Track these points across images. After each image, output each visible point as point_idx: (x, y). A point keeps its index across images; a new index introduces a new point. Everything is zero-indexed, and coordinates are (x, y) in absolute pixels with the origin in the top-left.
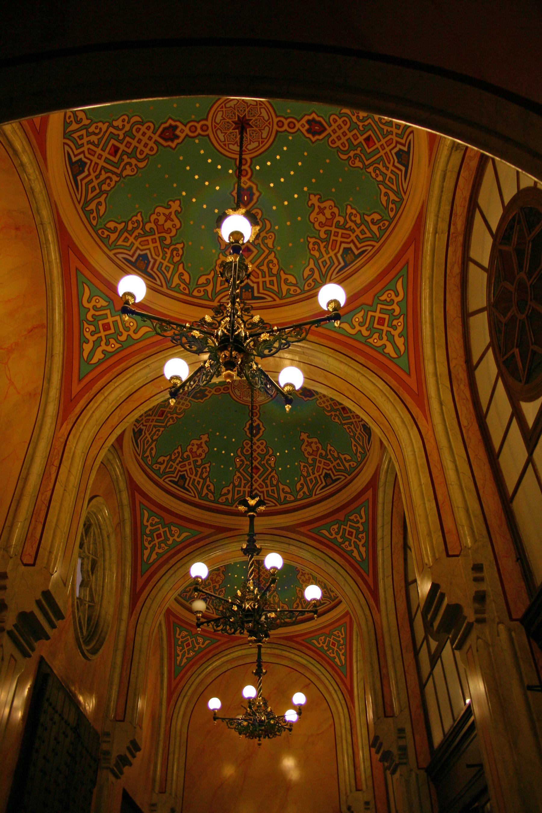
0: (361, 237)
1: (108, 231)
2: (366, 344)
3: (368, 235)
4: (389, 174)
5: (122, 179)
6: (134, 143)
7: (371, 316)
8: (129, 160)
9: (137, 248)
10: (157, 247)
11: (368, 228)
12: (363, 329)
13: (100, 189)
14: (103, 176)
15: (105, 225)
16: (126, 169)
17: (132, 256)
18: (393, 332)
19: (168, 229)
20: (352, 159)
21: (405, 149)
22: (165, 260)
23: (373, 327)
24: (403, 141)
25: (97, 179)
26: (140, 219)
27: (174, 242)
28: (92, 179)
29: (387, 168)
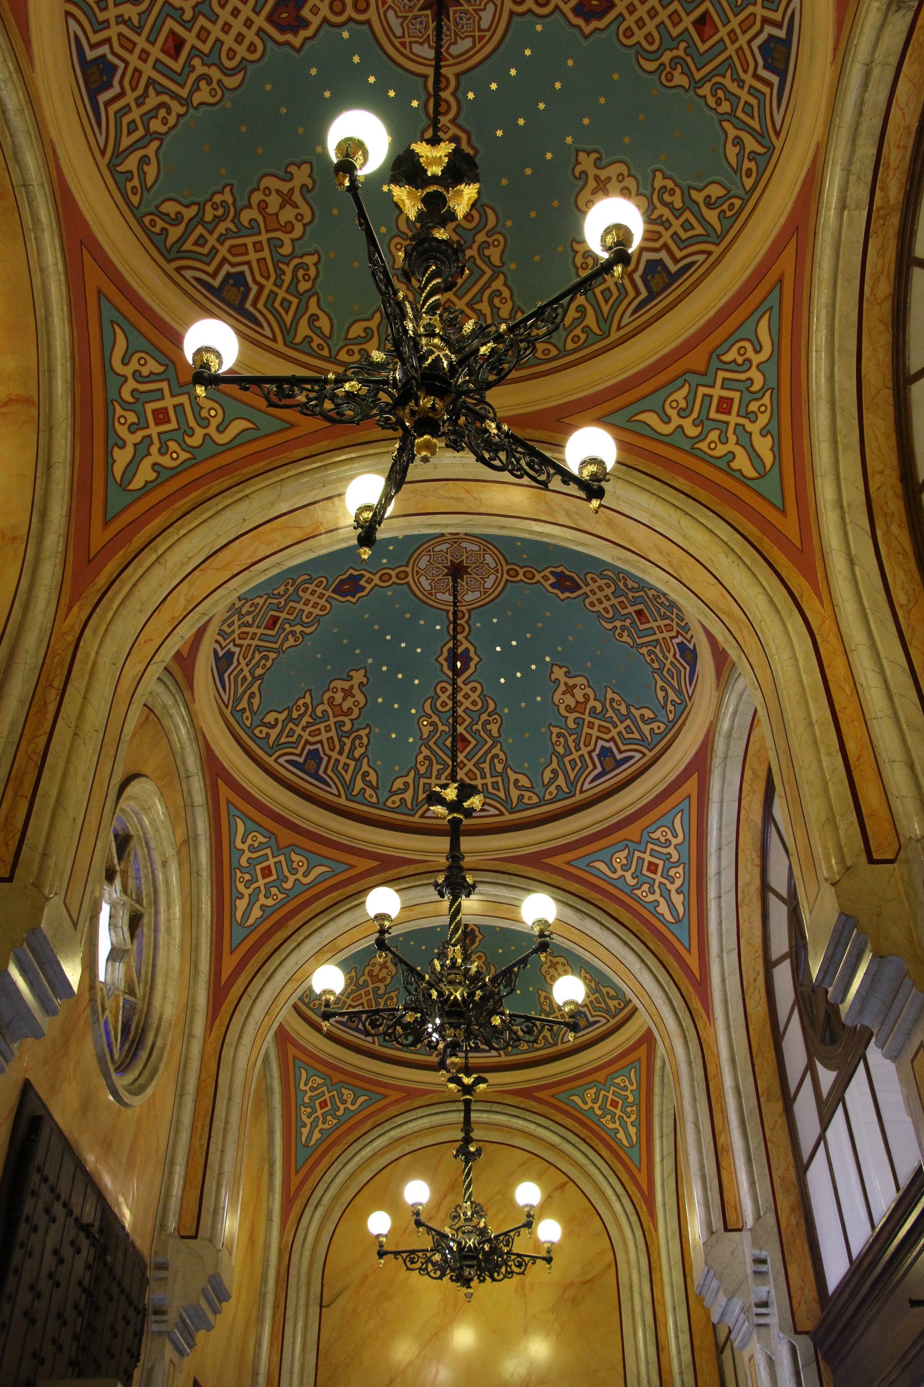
0: (684, 235)
1: (163, 220)
2: (693, 452)
3: (699, 230)
4: (744, 95)
5: (191, 110)
6: (216, 31)
7: (704, 395)
8: (205, 70)
9: (224, 260)
10: (264, 259)
11: (698, 215)
12: (687, 424)
13: (147, 128)
14: (153, 100)
15: (157, 208)
16: (198, 89)
17: (214, 276)
18: (749, 427)
19: (287, 223)
20: (668, 69)
21: (782, 34)
22: (280, 287)
23: (707, 419)
24: (777, 16)
25: (139, 106)
26: (230, 200)
27: (298, 252)
28: (128, 105)
29: (741, 83)
